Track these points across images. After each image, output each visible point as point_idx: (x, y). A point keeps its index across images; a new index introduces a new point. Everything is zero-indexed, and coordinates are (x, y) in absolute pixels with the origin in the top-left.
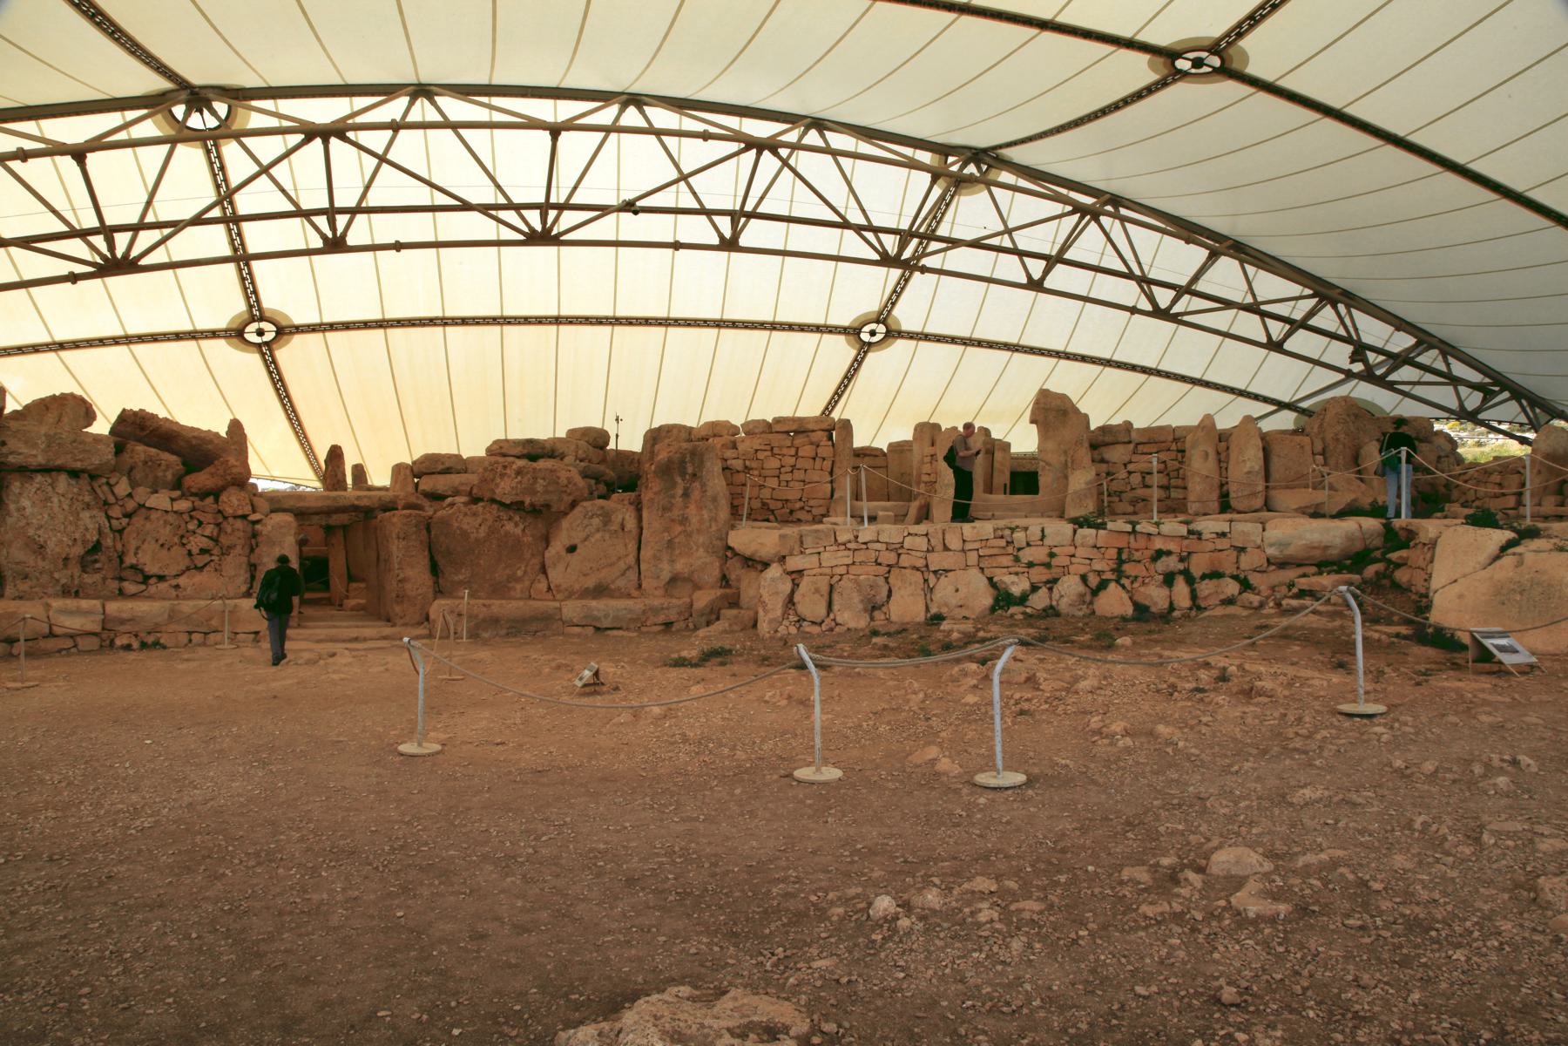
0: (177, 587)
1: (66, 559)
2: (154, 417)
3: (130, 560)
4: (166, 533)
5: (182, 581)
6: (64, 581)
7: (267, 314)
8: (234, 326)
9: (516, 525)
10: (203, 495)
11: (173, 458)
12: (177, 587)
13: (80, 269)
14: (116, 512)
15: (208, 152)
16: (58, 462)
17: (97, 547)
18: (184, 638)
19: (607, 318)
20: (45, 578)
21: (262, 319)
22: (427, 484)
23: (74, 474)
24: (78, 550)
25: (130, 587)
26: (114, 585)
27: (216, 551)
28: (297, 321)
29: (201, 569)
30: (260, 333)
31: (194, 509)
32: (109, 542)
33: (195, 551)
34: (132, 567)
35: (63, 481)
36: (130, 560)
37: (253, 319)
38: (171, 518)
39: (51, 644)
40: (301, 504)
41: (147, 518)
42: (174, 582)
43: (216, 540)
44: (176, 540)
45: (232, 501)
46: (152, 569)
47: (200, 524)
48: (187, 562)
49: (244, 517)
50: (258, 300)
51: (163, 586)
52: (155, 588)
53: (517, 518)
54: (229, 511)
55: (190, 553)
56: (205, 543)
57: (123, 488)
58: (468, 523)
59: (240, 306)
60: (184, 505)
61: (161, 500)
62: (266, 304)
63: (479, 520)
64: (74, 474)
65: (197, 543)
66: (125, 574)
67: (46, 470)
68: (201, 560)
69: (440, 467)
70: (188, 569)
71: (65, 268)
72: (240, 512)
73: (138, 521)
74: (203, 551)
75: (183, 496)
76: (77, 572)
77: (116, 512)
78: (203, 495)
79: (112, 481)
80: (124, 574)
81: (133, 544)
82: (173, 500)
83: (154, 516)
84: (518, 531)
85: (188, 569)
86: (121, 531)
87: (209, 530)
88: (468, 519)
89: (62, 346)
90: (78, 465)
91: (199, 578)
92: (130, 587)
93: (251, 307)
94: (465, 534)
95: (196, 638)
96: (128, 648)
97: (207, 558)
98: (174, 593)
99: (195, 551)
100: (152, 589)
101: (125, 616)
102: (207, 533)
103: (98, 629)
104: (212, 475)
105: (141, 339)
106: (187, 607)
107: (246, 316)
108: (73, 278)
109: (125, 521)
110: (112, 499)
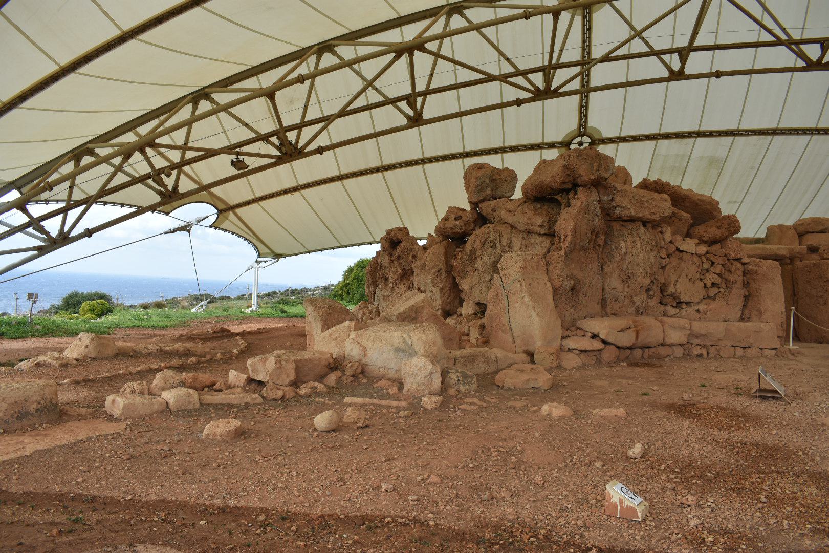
0: (698, 311)
2: (669, 184)
3: (671, 290)
4: (693, 270)
5: (702, 307)
6: (638, 303)
7: (589, 131)
8: (566, 140)
10: (712, 242)
11: (688, 215)
12: (698, 311)
14: (663, 254)
16: (641, 215)
19: (810, 129)
20: (627, 302)
21: (584, 135)
22: (812, 240)
24: (647, 281)
27: (723, 285)
28: (605, 135)
29: (714, 298)
30: (581, 144)
31: (707, 253)
33: (709, 284)
34: (672, 295)
35: (642, 230)
36: (671, 290)
37: (581, 134)
38: (696, 259)
39: (663, 351)
41: (681, 259)
42: (696, 308)
44: (698, 276)
46: (684, 297)
47: (713, 263)
48: (703, 293)
49: (738, 260)
50: (586, 122)
51: (690, 310)
55: (705, 286)
56: (716, 279)
57: (668, 236)
59: (574, 125)
61: (689, 245)
62: (591, 123)
64: (645, 224)
65: (711, 278)
67: (632, 220)
68: (713, 291)
69: (821, 228)
72: (739, 256)
73: (674, 260)
74: (713, 285)
76: (644, 296)
78: (712, 242)
79: (664, 230)
80: (664, 301)
87: (719, 269)
91: (713, 305)
92: (671, 311)
93: (580, 125)
96: (701, 356)
97: (716, 290)
98: (697, 315)
99: (709, 284)
100: (683, 312)
101: (703, 332)
102: (718, 271)
104: (719, 228)
107: (576, 132)
108: (519, 102)
110: (663, 245)
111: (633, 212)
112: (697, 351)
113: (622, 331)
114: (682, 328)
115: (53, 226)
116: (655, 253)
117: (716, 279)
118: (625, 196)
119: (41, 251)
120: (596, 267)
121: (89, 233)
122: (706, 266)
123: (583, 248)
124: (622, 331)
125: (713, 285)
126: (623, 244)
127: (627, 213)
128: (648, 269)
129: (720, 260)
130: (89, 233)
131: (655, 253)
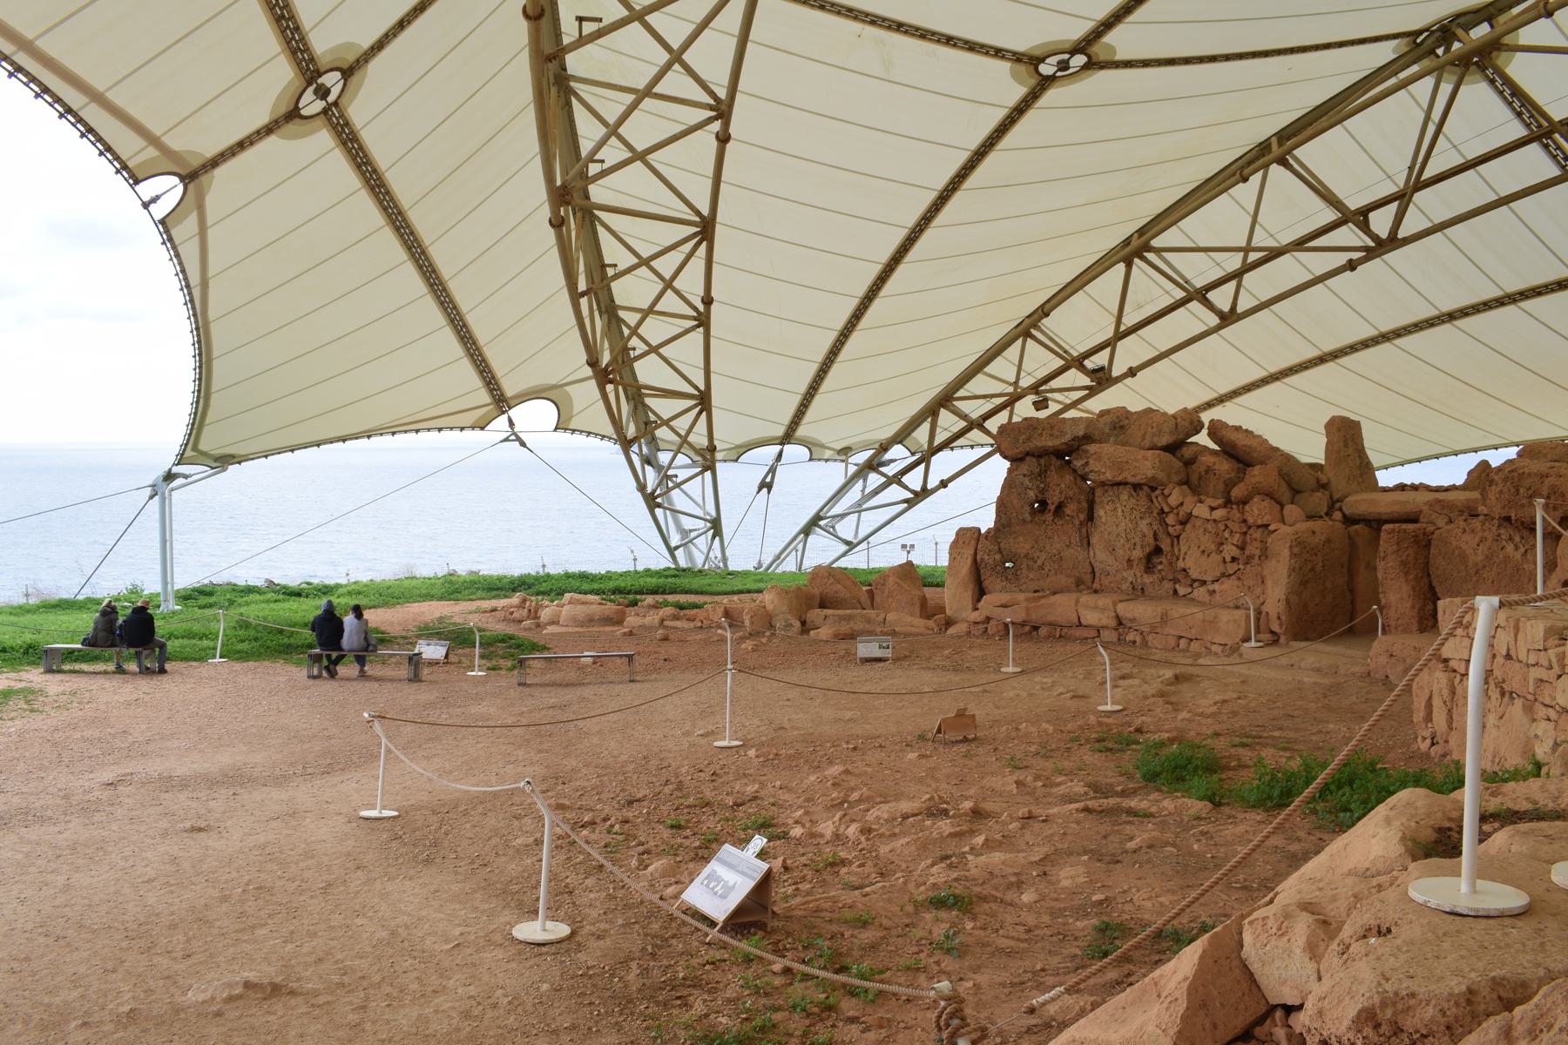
1: (1129, 560)
3: (1181, 564)
4: (1208, 542)
5: (1216, 586)
9: (1517, 548)
13: (1356, 255)
15: (1492, 82)
17: (1158, 551)
18: (1172, 642)
23: (1136, 487)
24: (1138, 553)
25: (1182, 591)
26: (1168, 585)
32: (1165, 546)
38: (1209, 526)
39: (1078, 632)
40: (1372, 509)
42: (1211, 588)
43: (1242, 548)
44: (1213, 547)
45: (1258, 510)
46: (1194, 574)
48: (1222, 568)
52: (1200, 593)
53: (1517, 539)
54: (1251, 521)
58: (1467, 542)
60: (1218, 514)
61: (1201, 511)
63: (1477, 540)
65: (1230, 550)
66: (1180, 576)
68: (1232, 568)
70: (1223, 575)
71: (1341, 259)
72: (1260, 522)
73: (1188, 526)
74: (1234, 559)
75: (1228, 502)
76: (1138, 570)
77: (1170, 520)
81: (1184, 549)
82: (1212, 509)
83: (1198, 523)
84: (1518, 555)
85: (1223, 575)
86: (1178, 537)
88: (1467, 537)
89: (1451, 317)
90: (1137, 480)
94: (1463, 557)
95: (1183, 643)
97: (1235, 566)
98: (1208, 598)
99: (1228, 559)
100: (1196, 593)
103: (1113, 623)
105: (1525, 295)
106: (1178, 610)
108: (1351, 266)
109: (1178, 527)
111: (1109, 476)
112: (1130, 637)
113: (1004, 606)
114: (1103, 610)
115: (914, 480)
116: (1148, 520)
117: (1236, 552)
118: (1099, 459)
119: (911, 503)
120: (1076, 538)
121: (944, 484)
122: (1226, 534)
123: (1024, 521)
124: (1004, 606)
125: (1234, 559)
126: (1102, 513)
127: (1102, 478)
128: (1137, 539)
129: (1235, 527)
130: (944, 484)
131: (1148, 520)
